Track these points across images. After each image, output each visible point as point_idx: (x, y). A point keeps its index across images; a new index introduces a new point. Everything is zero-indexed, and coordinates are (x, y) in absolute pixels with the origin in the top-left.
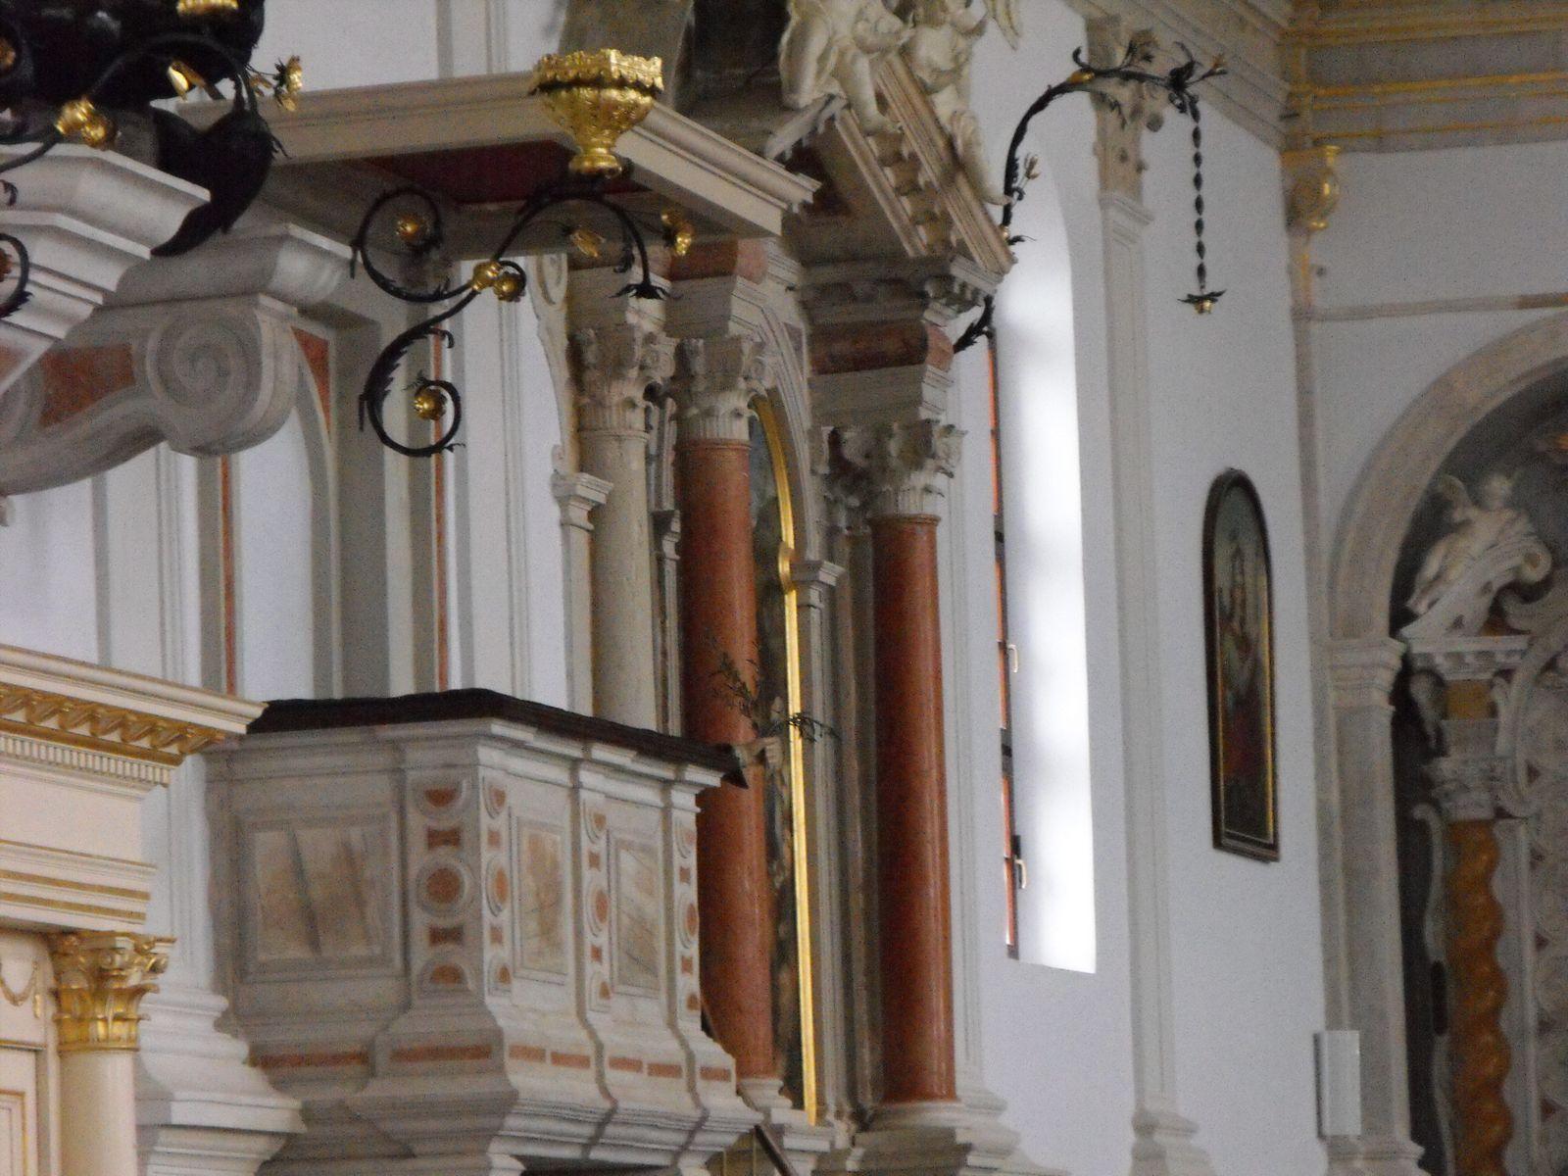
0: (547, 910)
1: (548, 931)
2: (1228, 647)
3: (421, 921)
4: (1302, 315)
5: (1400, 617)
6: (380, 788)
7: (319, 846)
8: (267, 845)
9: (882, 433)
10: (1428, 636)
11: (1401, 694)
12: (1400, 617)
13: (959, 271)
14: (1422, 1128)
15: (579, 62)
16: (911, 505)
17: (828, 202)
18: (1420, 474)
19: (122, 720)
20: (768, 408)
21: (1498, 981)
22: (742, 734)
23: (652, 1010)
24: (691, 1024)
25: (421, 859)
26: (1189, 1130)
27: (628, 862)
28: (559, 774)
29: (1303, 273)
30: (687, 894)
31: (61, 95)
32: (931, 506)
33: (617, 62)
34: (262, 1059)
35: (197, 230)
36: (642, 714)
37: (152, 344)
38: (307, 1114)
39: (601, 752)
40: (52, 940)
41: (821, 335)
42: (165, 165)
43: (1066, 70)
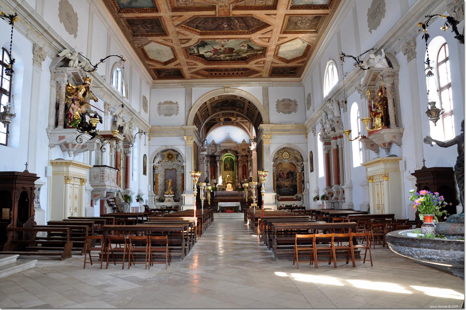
0: (108, 178)
1: (108, 179)
2: (144, 164)
3: (101, 178)
4: (149, 146)
5: (154, 162)
6: (99, 170)
7: (95, 174)
8: (92, 173)
9: (127, 151)
10: (155, 164)
11: (153, 167)
12: (154, 162)
13: (132, 143)
14: (154, 190)
15: (114, 131)
16: (128, 155)
17: (125, 139)
18: (155, 155)
19: (85, 166)
20: (121, 149)
21: (158, 182)
22: (119, 168)
23: (114, 183)
24: (116, 184)
25: (101, 175)
26: (141, 190)
27: (113, 175)
28: (109, 170)
29: (149, 143)
30: (116, 177)
31: (85, 130)
32: (129, 156)
33: (116, 131)
34: (91, 186)
35: (92, 138)
37: (88, 145)
38: (94, 189)
39: (112, 169)
40: (81, 179)
41: (124, 146)
42: (90, 135)
43: (138, 132)
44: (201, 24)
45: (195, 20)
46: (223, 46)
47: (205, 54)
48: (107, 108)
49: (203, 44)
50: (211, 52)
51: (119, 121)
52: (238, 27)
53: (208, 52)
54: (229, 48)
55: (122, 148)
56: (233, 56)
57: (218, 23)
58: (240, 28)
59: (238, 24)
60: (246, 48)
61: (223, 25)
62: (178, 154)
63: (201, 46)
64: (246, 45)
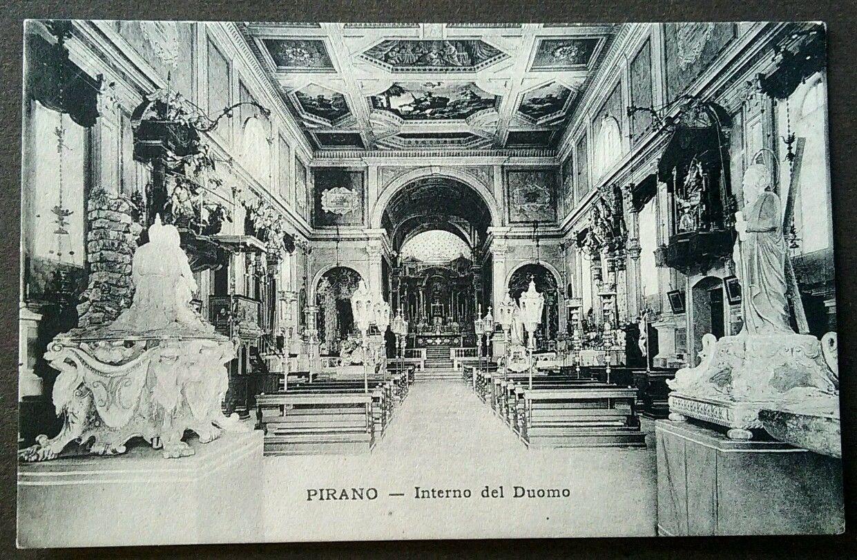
36: (252, 297)
44: (394, 53)
45: (384, 45)
46: (430, 94)
47: (399, 109)
48: (238, 197)
49: (397, 90)
50: (410, 105)
51: (258, 222)
52: (456, 59)
53: (405, 105)
54: (440, 98)
55: (265, 265)
56: (446, 112)
57: (422, 52)
58: (459, 60)
59: (456, 53)
60: (468, 98)
61: (431, 54)
62: (356, 277)
63: (394, 94)
64: (468, 92)
